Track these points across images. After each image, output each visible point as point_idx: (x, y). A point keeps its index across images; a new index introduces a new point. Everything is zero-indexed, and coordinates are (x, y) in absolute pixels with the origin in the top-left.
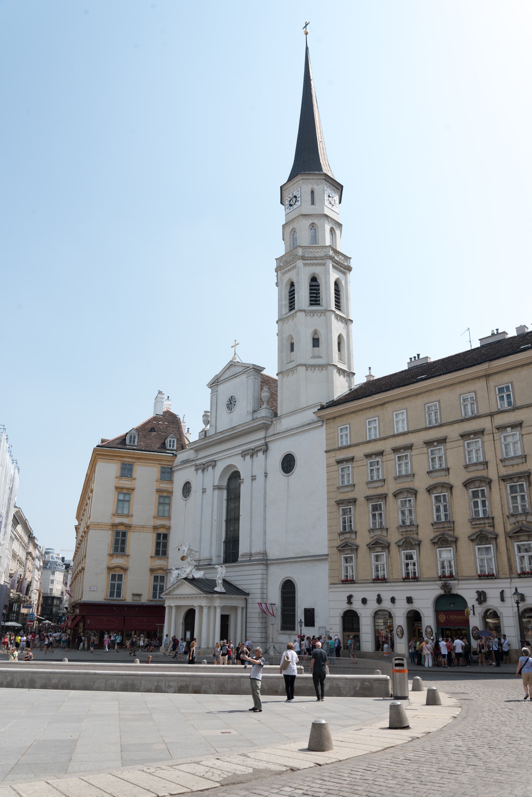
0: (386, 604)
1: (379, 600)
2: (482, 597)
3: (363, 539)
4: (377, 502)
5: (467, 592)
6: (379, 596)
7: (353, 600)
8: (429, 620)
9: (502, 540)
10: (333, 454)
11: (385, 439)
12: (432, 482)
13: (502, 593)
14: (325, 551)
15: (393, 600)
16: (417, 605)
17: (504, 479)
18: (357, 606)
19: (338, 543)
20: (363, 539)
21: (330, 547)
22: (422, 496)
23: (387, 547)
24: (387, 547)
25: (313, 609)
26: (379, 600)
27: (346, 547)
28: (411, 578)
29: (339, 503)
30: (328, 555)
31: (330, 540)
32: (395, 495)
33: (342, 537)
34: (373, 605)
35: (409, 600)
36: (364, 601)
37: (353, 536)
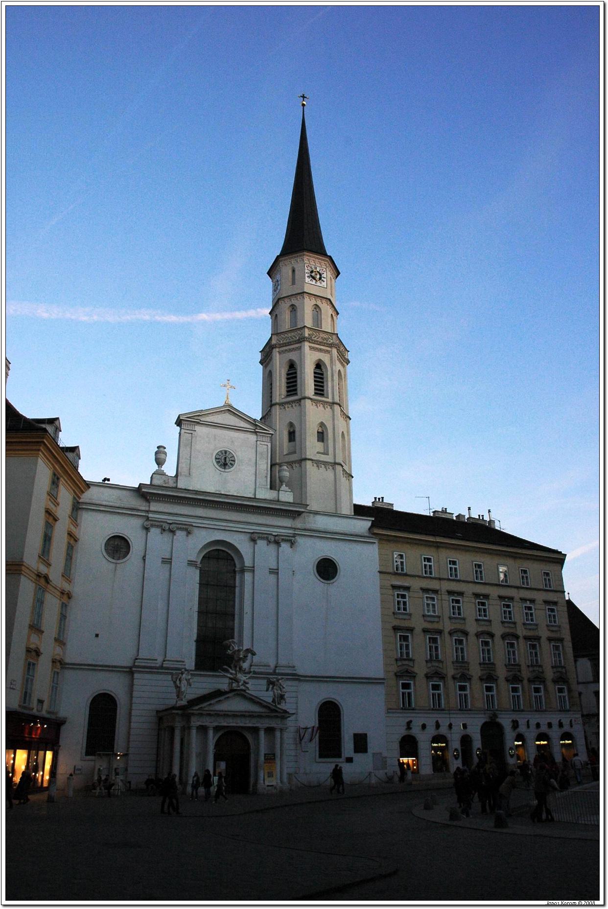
0: (443, 730)
1: (438, 726)
2: (515, 725)
3: (421, 669)
4: (433, 635)
5: (505, 721)
6: (437, 722)
7: (411, 725)
8: (477, 744)
9: (525, 682)
10: (388, 577)
11: (440, 579)
12: (480, 629)
13: (528, 722)
14: (382, 676)
15: (450, 726)
16: (469, 731)
17: (525, 638)
18: (416, 731)
19: (394, 668)
20: (421, 669)
21: (386, 672)
22: (472, 638)
23: (442, 677)
24: (442, 677)
25: (366, 735)
26: (438, 726)
27: (404, 673)
28: (464, 708)
29: (396, 629)
30: (383, 679)
31: (386, 665)
32: (451, 633)
33: (400, 663)
34: (431, 731)
35: (465, 726)
36: (424, 727)
37: (411, 664)
